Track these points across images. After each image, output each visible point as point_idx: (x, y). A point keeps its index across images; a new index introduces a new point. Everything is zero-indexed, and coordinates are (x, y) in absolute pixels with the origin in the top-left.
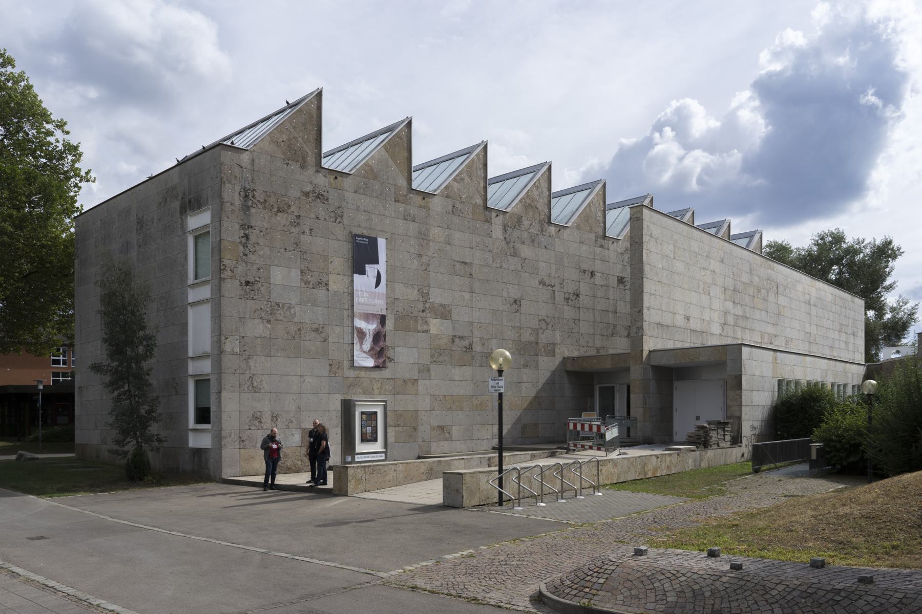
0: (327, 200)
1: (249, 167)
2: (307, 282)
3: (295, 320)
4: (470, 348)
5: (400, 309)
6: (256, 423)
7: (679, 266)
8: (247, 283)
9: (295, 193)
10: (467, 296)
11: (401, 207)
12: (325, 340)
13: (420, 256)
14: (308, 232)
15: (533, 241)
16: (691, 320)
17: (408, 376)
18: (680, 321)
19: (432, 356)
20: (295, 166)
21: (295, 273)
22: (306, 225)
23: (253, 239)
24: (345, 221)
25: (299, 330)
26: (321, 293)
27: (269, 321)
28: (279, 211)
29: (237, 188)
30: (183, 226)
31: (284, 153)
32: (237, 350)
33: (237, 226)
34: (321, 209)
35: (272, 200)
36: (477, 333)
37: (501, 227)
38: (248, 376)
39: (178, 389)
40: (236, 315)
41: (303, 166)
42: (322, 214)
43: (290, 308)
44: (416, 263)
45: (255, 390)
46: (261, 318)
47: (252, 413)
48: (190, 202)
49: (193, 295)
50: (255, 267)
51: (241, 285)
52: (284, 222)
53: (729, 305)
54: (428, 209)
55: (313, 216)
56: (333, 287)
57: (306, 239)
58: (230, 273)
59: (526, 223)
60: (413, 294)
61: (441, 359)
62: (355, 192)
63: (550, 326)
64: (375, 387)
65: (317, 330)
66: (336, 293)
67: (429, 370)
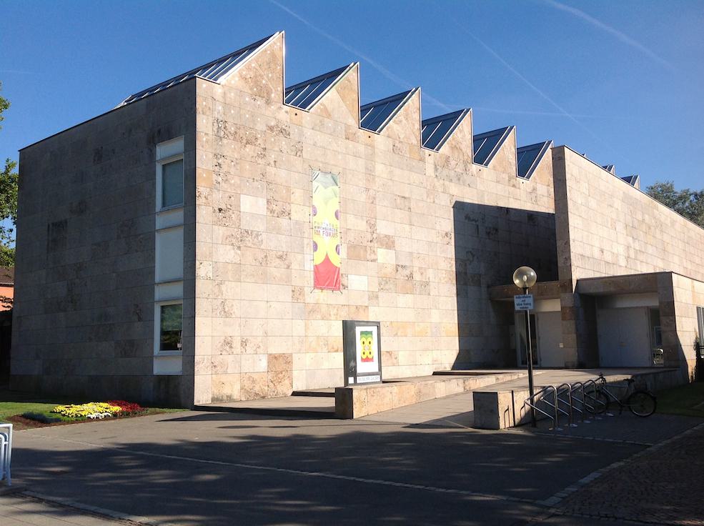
0: (289, 134)
1: (221, 100)
2: (272, 211)
3: (262, 247)
4: (411, 276)
5: (352, 239)
6: (227, 348)
7: (593, 204)
8: (220, 210)
9: (261, 127)
10: (407, 227)
11: (351, 144)
12: (288, 267)
13: (367, 190)
14: (273, 163)
15: (459, 179)
16: (605, 252)
17: (359, 303)
18: (597, 254)
19: (380, 284)
20: (260, 102)
21: (262, 202)
22: (272, 157)
23: (225, 168)
24: (305, 155)
25: (266, 256)
26: (284, 222)
27: (239, 248)
28: (247, 143)
29: (211, 119)
30: (152, 155)
31: (251, 89)
32: (210, 275)
33: (211, 156)
34: (283, 143)
35: (241, 132)
36: (417, 264)
37: (433, 166)
38: (220, 301)
39: (143, 314)
40: (209, 241)
41: (268, 102)
42: (284, 147)
43: (257, 235)
44: (364, 196)
45: (227, 314)
46: (232, 244)
47: (223, 338)
48: (159, 131)
49: (160, 221)
50: (227, 195)
51: (214, 211)
52: (252, 153)
53: (630, 239)
54: (373, 147)
55: (277, 149)
56: (294, 216)
57: (271, 170)
58: (204, 200)
59: (453, 163)
60: (362, 226)
61: (387, 287)
62: (313, 129)
63: (475, 257)
64: (332, 313)
65: (280, 257)
66: (297, 222)
67: (377, 297)
